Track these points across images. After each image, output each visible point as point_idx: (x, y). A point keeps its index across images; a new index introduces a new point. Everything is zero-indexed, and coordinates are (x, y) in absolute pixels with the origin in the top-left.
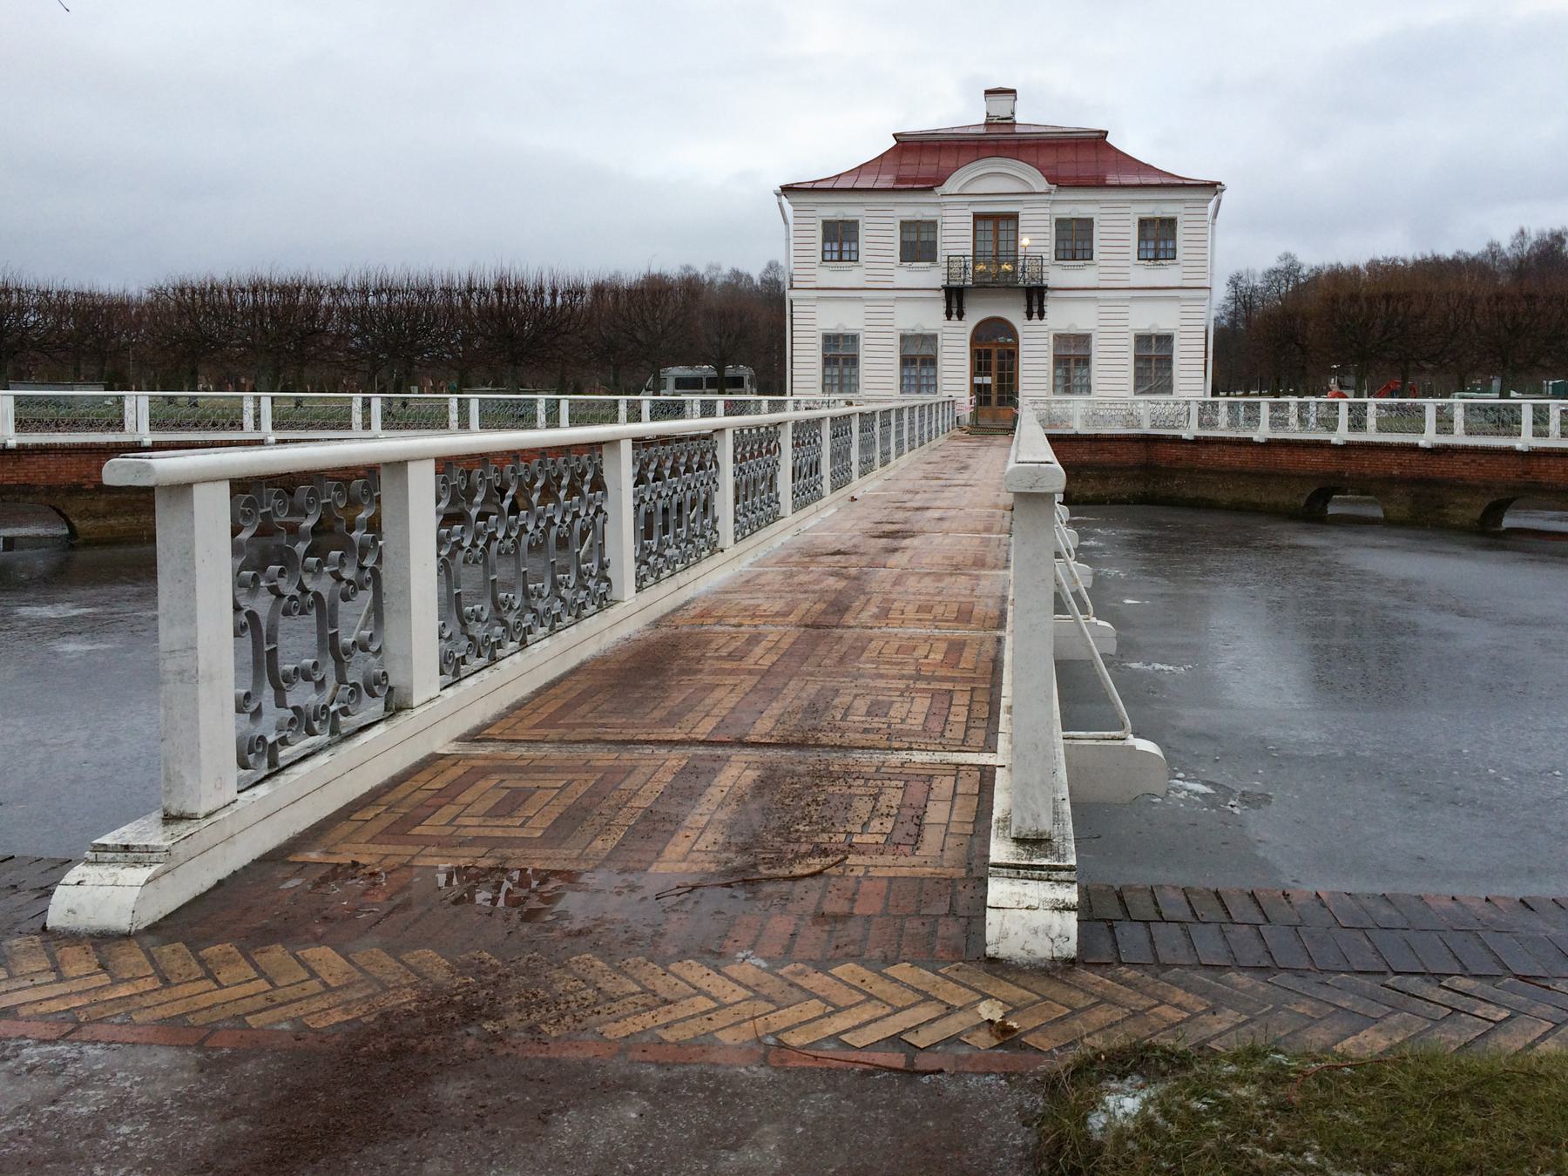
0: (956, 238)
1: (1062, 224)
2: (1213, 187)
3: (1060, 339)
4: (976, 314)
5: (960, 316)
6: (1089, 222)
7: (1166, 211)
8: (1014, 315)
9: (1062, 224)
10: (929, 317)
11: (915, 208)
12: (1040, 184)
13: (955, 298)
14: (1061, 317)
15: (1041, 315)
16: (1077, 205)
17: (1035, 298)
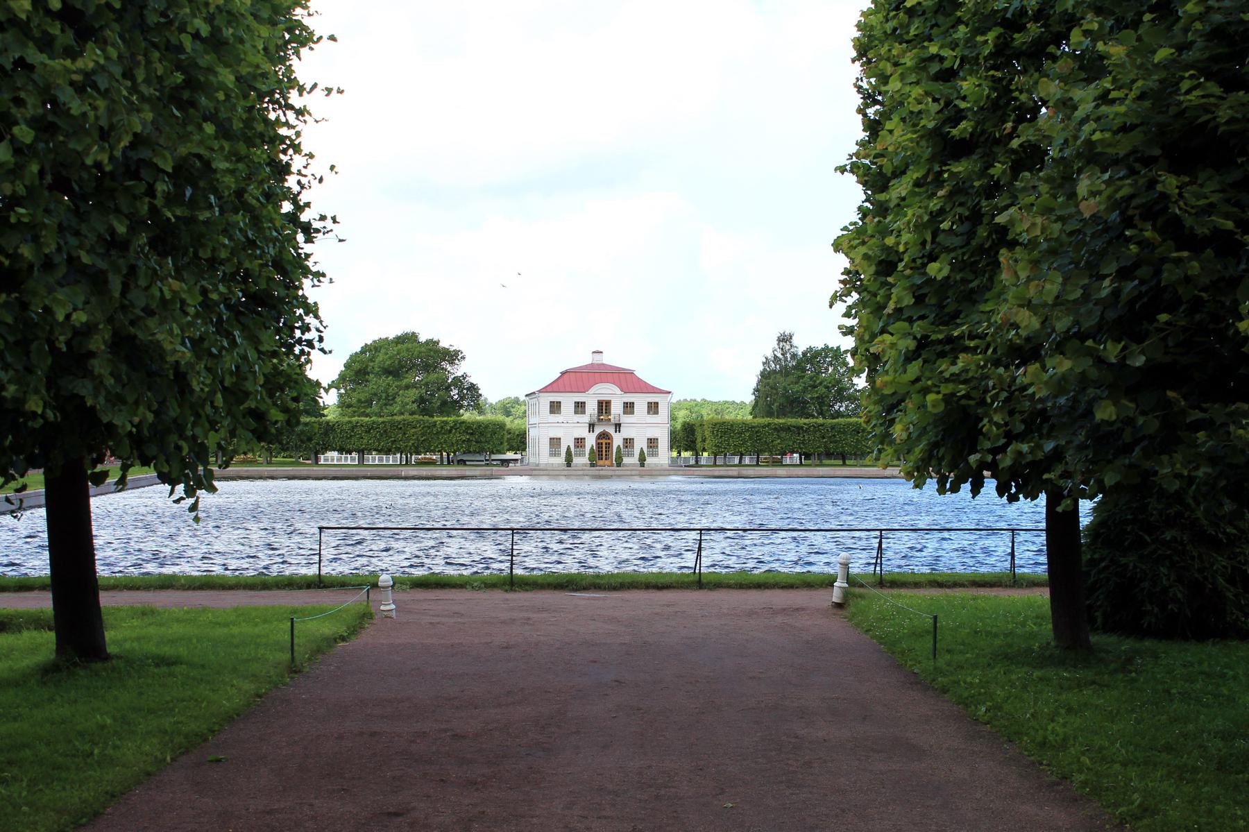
0: (592, 408)
1: (626, 404)
2: (670, 392)
3: (626, 440)
5: (593, 431)
6: (633, 403)
7: (656, 400)
9: (626, 404)
10: (583, 432)
11: (579, 397)
12: (618, 391)
13: (592, 426)
14: (626, 432)
15: (619, 431)
16: (629, 398)
17: (618, 426)
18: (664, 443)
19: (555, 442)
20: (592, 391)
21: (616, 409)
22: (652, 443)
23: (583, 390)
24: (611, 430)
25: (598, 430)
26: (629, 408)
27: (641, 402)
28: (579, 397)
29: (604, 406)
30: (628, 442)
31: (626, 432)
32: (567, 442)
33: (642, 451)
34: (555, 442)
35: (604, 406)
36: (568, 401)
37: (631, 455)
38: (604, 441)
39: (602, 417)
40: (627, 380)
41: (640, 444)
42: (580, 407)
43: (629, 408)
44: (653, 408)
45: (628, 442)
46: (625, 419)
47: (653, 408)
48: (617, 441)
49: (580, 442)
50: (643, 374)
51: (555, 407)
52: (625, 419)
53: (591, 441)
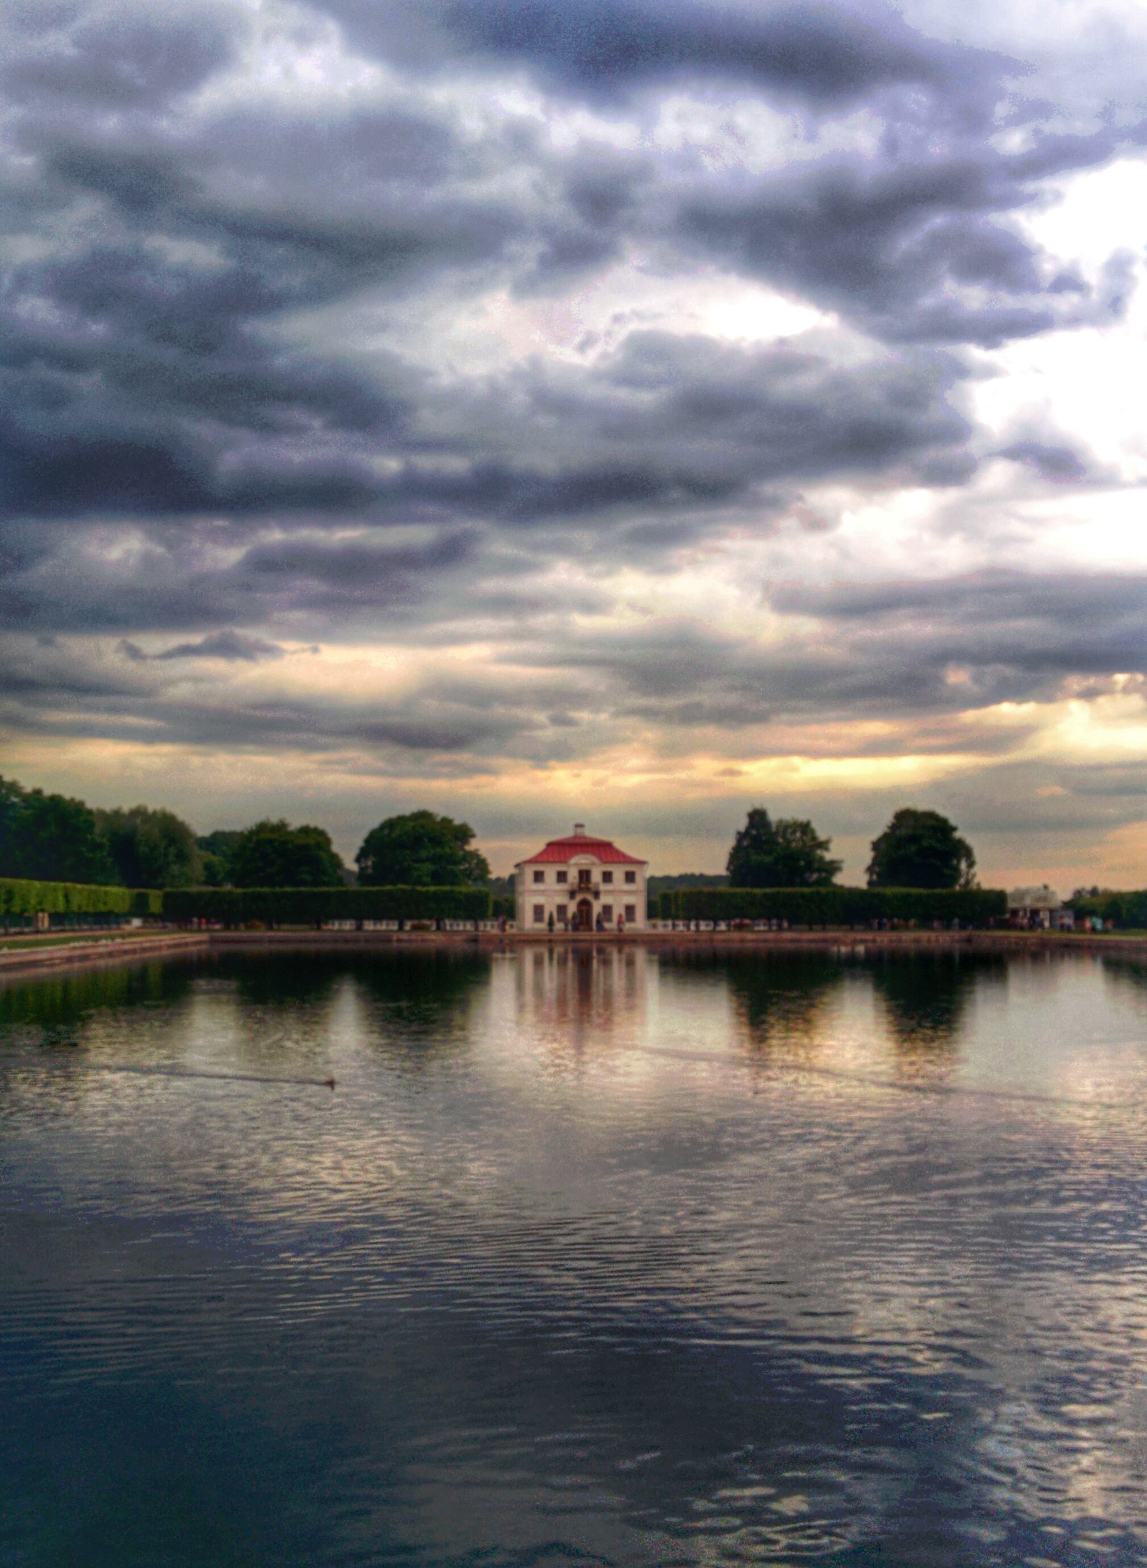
0: (573, 875)
4: (579, 897)
8: (590, 897)
11: (561, 868)
13: (572, 894)
14: (605, 900)
17: (597, 894)
18: (640, 912)
19: (538, 910)
20: (573, 861)
21: (596, 877)
22: (630, 910)
23: (564, 861)
24: (590, 897)
25: (579, 897)
26: (607, 877)
27: (618, 872)
28: (561, 868)
29: (585, 875)
30: (607, 909)
31: (605, 900)
32: (550, 908)
33: (620, 916)
34: (538, 910)
35: (585, 875)
36: (550, 872)
37: (609, 920)
38: (584, 908)
39: (583, 886)
40: (603, 849)
41: (618, 911)
42: (562, 877)
43: (607, 877)
44: (630, 877)
45: (607, 909)
46: (603, 887)
47: (630, 877)
48: (597, 908)
49: (562, 909)
50: (620, 844)
51: (539, 877)
52: (603, 887)
53: (572, 908)
